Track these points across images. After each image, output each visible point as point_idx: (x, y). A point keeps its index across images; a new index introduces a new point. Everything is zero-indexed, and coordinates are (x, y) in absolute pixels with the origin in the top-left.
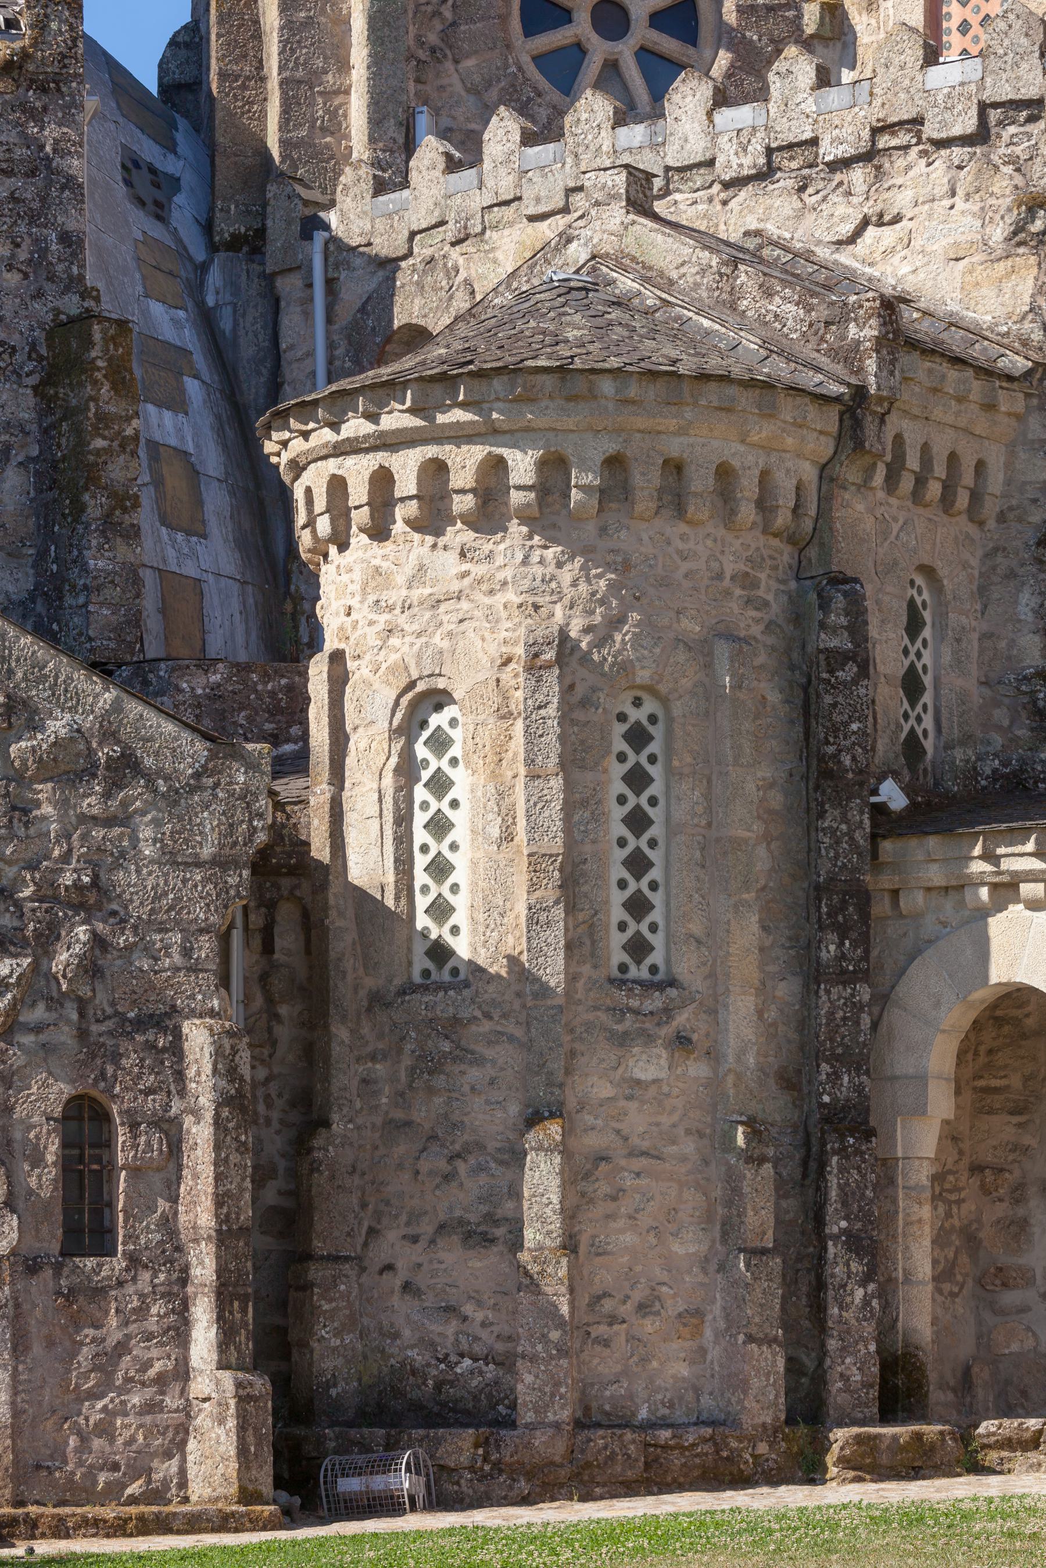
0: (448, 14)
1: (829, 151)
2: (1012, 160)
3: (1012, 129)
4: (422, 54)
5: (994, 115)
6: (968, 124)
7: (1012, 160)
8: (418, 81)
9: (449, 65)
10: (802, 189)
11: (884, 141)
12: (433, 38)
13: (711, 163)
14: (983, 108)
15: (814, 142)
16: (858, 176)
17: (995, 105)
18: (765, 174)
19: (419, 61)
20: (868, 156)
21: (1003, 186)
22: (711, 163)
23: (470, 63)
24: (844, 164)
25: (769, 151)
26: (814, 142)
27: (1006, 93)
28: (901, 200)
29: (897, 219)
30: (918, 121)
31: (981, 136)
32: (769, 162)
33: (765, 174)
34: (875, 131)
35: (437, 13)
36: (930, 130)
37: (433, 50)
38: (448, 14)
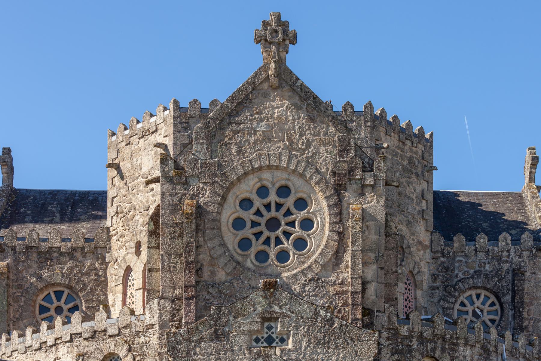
0: (20, 311)
1: (49, 344)
2: (76, 346)
3: (77, 339)
4: (14, 320)
5: (73, 336)
6: (68, 338)
7: (76, 346)
8: (13, 325)
9: (21, 322)
10: (46, 352)
11: (58, 342)
12: (17, 316)
13: (32, 346)
14: (71, 335)
15: (46, 342)
16: (54, 349)
17: (74, 334)
18: (40, 348)
19: (14, 321)
20: (55, 345)
21: (75, 351)
22: (32, 346)
23: (25, 321)
24: (51, 346)
25: (41, 344)
26: (46, 342)
27: (75, 332)
28: (60, 354)
29: (60, 358)
30: (61, 337)
31: (71, 341)
32: (41, 346)
33: (40, 348)
34: (56, 340)
35: (18, 311)
36: (64, 340)
37: (17, 319)
38: (20, 311)
